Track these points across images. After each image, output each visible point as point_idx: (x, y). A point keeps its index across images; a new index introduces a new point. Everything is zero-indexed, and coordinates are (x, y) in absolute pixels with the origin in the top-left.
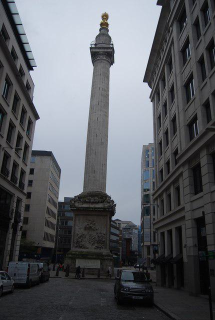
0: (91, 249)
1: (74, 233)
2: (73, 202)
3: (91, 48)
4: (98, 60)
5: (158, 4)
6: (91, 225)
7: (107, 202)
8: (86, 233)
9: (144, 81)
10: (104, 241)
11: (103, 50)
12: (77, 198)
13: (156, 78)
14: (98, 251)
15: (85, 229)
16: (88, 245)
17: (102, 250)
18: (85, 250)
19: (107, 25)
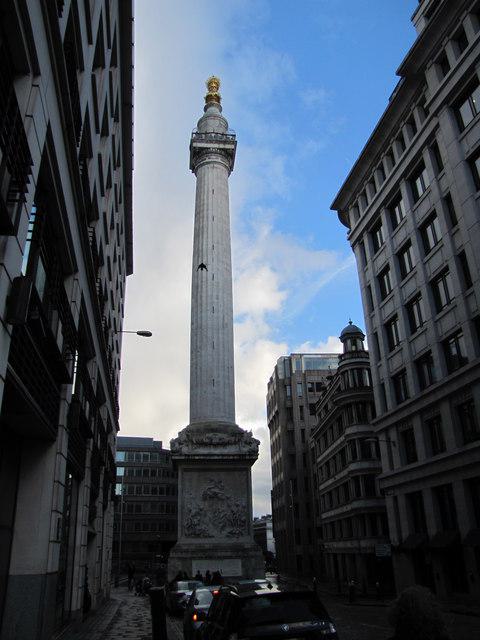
0: (220, 538)
1: (183, 508)
2: (177, 445)
3: (192, 141)
4: (207, 163)
5: (398, 74)
6: (217, 490)
7: (246, 443)
8: (204, 505)
9: (333, 207)
10: (244, 522)
11: (216, 146)
12: (185, 436)
13: (374, 200)
14: (234, 540)
15: (205, 499)
16: (212, 531)
17: (242, 540)
18: (206, 542)
19: (218, 99)
